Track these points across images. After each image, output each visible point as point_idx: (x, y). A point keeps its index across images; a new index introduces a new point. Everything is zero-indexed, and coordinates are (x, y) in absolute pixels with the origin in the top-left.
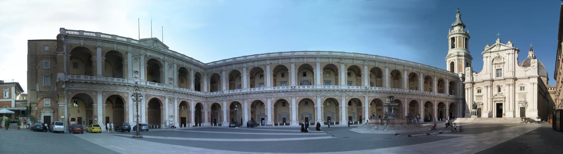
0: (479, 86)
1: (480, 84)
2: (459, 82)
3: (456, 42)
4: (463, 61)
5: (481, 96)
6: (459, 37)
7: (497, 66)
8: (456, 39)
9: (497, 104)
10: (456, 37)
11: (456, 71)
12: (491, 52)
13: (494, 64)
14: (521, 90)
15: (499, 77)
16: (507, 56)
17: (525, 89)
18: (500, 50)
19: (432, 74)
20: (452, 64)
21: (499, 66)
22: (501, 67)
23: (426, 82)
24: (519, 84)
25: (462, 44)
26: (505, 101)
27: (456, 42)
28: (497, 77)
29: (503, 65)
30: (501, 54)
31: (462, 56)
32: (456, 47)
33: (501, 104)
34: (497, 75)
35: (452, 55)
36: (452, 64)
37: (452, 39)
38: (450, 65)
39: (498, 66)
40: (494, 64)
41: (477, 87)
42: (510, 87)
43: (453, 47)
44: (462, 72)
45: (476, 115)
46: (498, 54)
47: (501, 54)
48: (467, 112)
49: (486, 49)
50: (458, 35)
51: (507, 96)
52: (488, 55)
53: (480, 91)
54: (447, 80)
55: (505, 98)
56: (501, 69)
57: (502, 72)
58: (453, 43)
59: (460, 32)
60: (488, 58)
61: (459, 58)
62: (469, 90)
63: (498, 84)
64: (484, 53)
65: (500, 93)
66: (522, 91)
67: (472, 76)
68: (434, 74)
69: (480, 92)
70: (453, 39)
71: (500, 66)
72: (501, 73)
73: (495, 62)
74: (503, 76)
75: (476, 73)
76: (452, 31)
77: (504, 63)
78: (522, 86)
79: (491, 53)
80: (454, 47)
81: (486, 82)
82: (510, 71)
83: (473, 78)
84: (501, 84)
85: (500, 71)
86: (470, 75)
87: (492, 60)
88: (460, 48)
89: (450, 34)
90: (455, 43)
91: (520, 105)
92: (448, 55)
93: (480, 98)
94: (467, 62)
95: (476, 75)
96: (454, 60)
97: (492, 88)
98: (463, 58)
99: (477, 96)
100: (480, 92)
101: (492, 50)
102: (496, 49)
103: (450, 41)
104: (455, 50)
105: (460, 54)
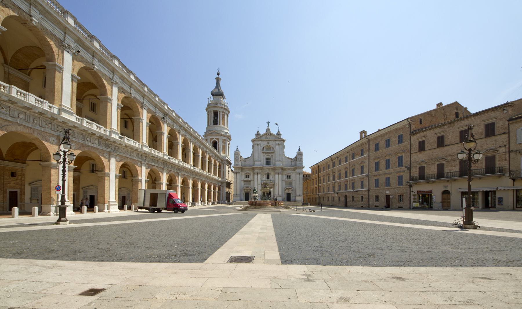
0: (248, 171)
2: (223, 165)
5: (250, 181)
7: (266, 154)
8: (220, 114)
10: (220, 112)
13: (263, 153)
14: (287, 178)
16: (277, 146)
17: (291, 178)
21: (269, 155)
28: (266, 165)
29: (272, 154)
32: (220, 125)
34: (266, 163)
39: (267, 154)
40: (263, 153)
41: (245, 173)
46: (268, 143)
53: (249, 176)
55: (274, 185)
60: (259, 146)
69: (249, 178)
72: (270, 161)
73: (265, 150)
74: (272, 165)
79: (262, 141)
85: (269, 160)
87: (262, 148)
93: (248, 183)
96: (218, 139)
99: (245, 181)
100: (249, 178)
102: (266, 138)
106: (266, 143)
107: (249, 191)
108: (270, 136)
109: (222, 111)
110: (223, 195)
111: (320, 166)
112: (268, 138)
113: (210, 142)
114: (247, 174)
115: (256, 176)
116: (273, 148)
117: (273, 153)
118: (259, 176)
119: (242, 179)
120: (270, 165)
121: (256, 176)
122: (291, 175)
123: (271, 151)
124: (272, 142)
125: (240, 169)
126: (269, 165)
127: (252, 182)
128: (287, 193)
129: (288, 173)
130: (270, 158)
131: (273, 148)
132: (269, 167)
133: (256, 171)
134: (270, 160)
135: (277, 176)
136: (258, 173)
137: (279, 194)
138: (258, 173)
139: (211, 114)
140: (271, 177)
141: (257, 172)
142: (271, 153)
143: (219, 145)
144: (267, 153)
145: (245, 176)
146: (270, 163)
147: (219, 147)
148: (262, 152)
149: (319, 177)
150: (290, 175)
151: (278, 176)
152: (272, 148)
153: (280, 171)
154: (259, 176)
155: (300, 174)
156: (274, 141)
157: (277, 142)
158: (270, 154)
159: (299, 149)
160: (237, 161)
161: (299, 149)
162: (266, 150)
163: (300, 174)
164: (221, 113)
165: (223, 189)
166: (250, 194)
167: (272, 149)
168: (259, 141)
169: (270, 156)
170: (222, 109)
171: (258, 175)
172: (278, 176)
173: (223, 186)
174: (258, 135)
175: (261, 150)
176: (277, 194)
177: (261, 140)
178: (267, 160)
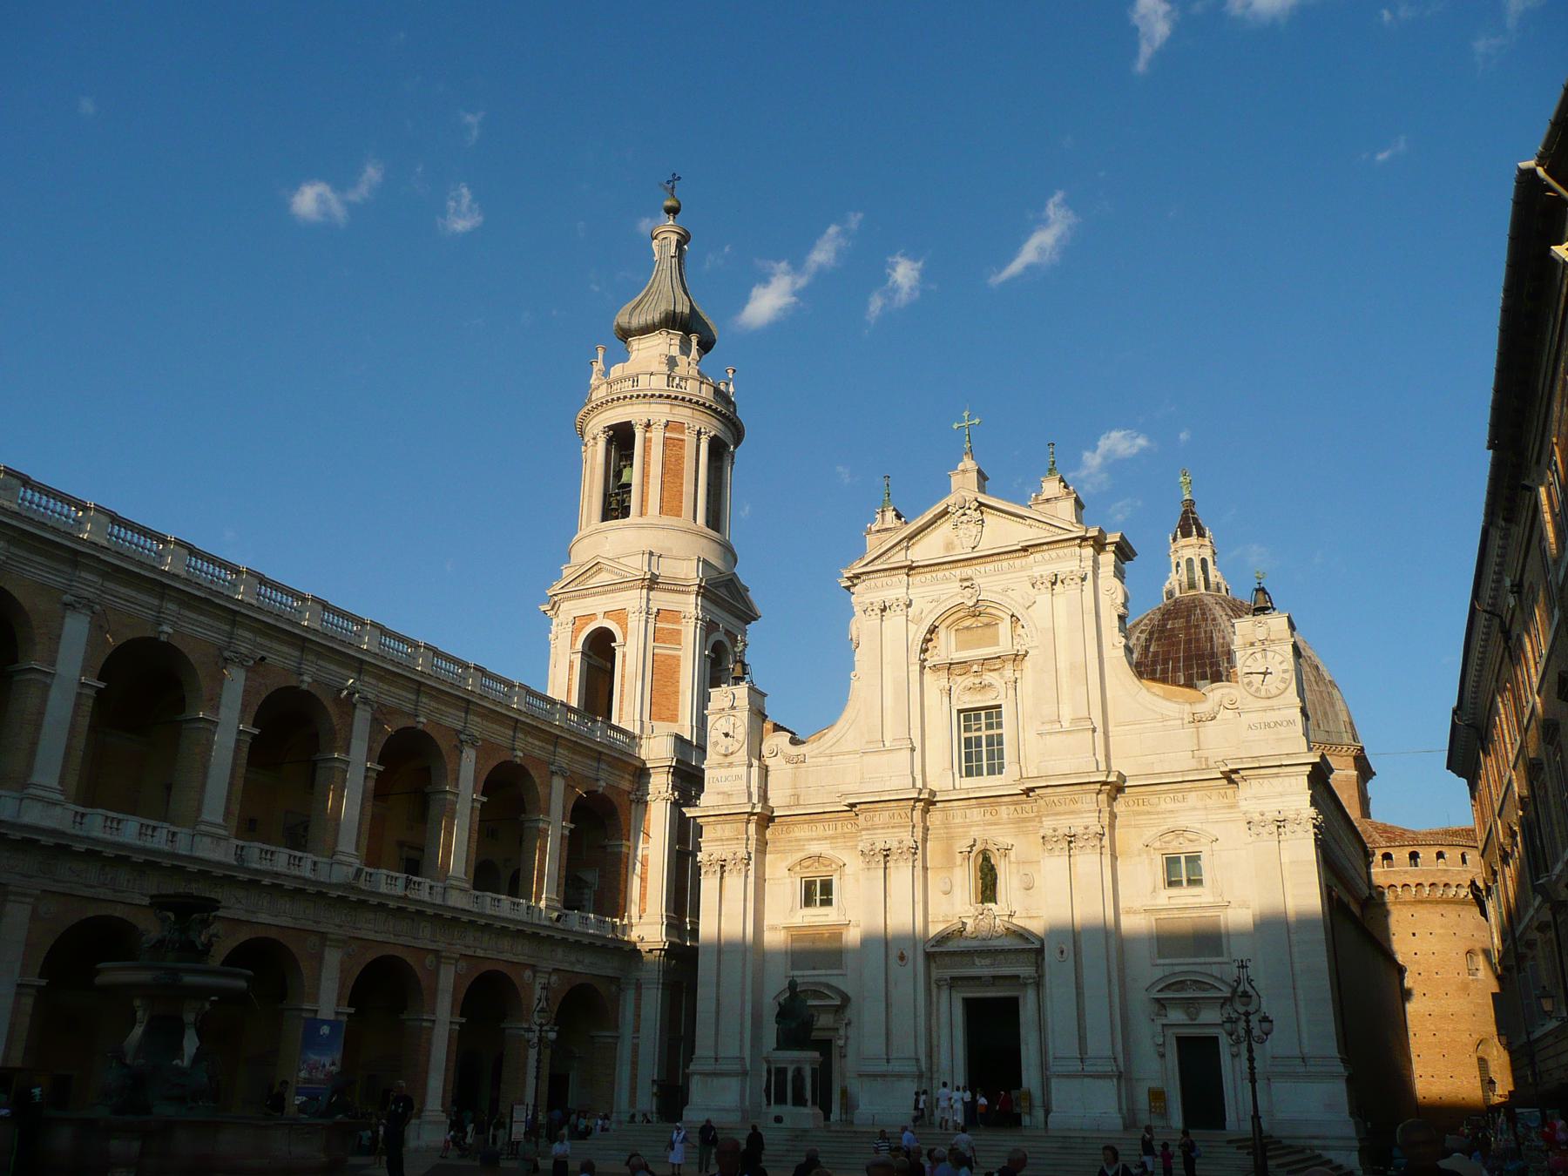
0: (815, 848)
1: (819, 830)
4: (690, 633)
6: (667, 425)
8: (647, 441)
9: (968, 1003)
11: (627, 710)
12: (910, 569)
13: (935, 668)
15: (980, 774)
16: (1043, 597)
18: (985, 547)
19: (448, 721)
20: (600, 649)
23: (381, 790)
24: (1149, 834)
25: (688, 488)
26: (1039, 983)
28: (969, 773)
29: (1008, 672)
30: (992, 583)
31: (677, 588)
33: (1010, 1008)
34: (968, 757)
35: (604, 577)
36: (600, 649)
37: (609, 442)
38: (577, 659)
39: (970, 680)
40: (935, 668)
41: (802, 855)
43: (616, 505)
44: (673, 718)
45: (804, 1104)
47: (992, 583)
48: (708, 1068)
49: (874, 545)
50: (661, 413)
52: (893, 589)
53: (827, 887)
54: (558, 785)
56: (999, 706)
57: (1007, 731)
58: (619, 475)
59: (673, 392)
60: (895, 620)
61: (661, 600)
62: (734, 882)
63: (975, 832)
64: (857, 576)
65: (991, 905)
67: (760, 757)
68: (459, 726)
69: (827, 902)
70: (621, 439)
71: (990, 685)
72: (1001, 735)
73: (947, 647)
74: (1010, 770)
75: (795, 741)
76: (617, 370)
77: (1018, 658)
78: (1182, 847)
79: (916, 579)
80: (625, 512)
81: (882, 817)
82: (1066, 724)
83: (765, 771)
84: (1000, 836)
85: (989, 726)
86: (742, 755)
88: (667, 520)
89: (600, 394)
90: (634, 475)
91: (1176, 1016)
92: (568, 572)
94: (716, 637)
95: (795, 750)
96: (620, 615)
97: (925, 869)
98: (690, 605)
100: (827, 902)
101: (925, 550)
102: (949, 546)
103: (595, 454)
104: (630, 534)
105: (666, 569)
106: (955, 586)
110: (634, 1064)
113: (572, 645)
114: (809, 874)
117: (1018, 658)
122: (1204, 848)
126: (991, 772)
128: (1182, 1042)
130: (994, 711)
132: (985, 783)
134: (1000, 725)
137: (1091, 1050)
140: (1007, 881)
141: (880, 845)
143: (624, 656)
147: (623, 676)
150: (1191, 848)
153: (1086, 815)
156: (1017, 562)
158: (989, 677)
160: (730, 765)
165: (638, 1007)
167: (1004, 627)
169: (997, 689)
170: (666, 408)
173: (639, 987)
178: (979, 729)
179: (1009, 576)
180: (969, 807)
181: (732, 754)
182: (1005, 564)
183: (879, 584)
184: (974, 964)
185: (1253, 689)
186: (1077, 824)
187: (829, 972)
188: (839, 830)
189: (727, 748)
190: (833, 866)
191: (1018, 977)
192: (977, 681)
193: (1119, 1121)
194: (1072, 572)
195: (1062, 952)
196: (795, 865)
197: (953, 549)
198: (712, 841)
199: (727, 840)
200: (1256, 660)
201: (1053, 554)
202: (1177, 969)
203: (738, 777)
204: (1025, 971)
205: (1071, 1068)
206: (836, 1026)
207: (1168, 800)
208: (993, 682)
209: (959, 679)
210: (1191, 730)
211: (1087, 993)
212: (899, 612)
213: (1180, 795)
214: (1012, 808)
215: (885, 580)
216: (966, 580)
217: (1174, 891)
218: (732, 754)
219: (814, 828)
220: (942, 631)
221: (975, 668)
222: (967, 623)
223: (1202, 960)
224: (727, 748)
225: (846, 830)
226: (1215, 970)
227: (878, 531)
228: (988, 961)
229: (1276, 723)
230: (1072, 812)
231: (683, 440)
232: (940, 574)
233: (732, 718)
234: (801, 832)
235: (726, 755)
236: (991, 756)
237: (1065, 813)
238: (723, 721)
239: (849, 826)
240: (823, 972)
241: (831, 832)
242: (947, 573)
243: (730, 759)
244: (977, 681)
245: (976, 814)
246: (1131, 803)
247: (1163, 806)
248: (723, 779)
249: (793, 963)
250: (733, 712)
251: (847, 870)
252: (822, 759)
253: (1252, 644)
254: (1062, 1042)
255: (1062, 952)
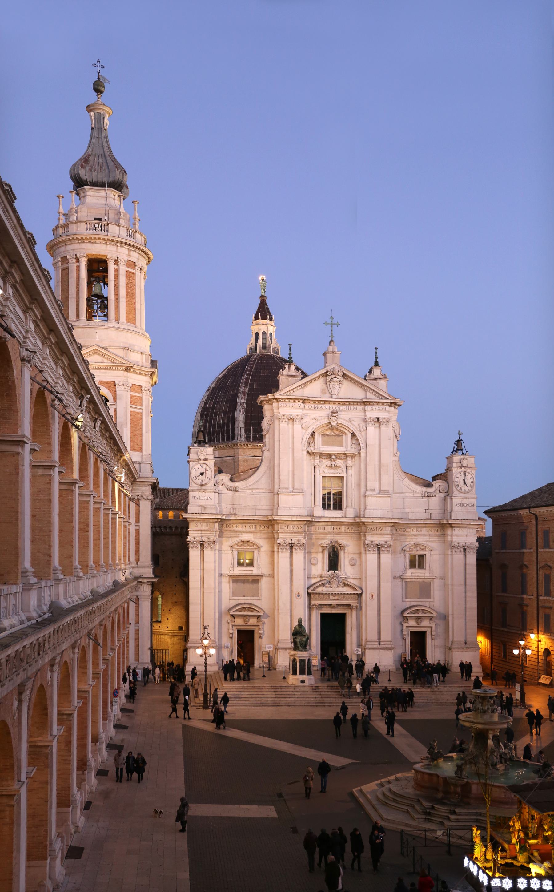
0: (245, 537)
1: (247, 528)
3: (117, 287)
5: (256, 580)
8: (117, 271)
9: (323, 615)
10: (117, 262)
16: (372, 430)
17: (427, 565)
22: (339, 471)
26: (359, 608)
27: (117, 287)
29: (350, 462)
32: (117, 320)
33: (340, 619)
39: (327, 462)
41: (239, 539)
42: (382, 555)
51: (370, 586)
52: (296, 410)
60: (297, 426)
66: (417, 573)
71: (339, 466)
93: (248, 586)
107: (253, 621)
108: (340, 383)
109: (126, 258)
111: (545, 520)
112: (335, 392)
115: (283, 557)
116: (353, 435)
117: (353, 456)
118: (299, 556)
119: (225, 571)
120: (340, 507)
121: (283, 557)
122: (427, 552)
123: (348, 447)
124: (348, 410)
125: (217, 525)
126: (335, 508)
127: (264, 583)
129: (416, 545)
131: (353, 435)
133: (284, 537)
135: (371, 557)
136: (291, 546)
137: (382, 638)
138: (291, 546)
139: (78, 268)
142: (346, 456)
144: (329, 456)
145: (235, 552)
146: (340, 500)
148: (308, 452)
149: (541, 565)
150: (421, 552)
151: (379, 558)
152: (349, 435)
154: (299, 556)
155: (465, 550)
156: (358, 407)
157: (372, 412)
158: (339, 462)
159: (459, 442)
160: (205, 491)
161: (459, 442)
162: (325, 444)
163: (465, 550)
164: (123, 269)
166: (256, 636)
168: (296, 404)
170: (126, 251)
171: (294, 554)
172: (379, 558)
174: (290, 378)
175: (305, 441)
176: (376, 638)
177: (305, 401)
179: (353, 413)
180: (327, 525)
181: (206, 484)
182: (352, 407)
183: (288, 405)
184: (329, 599)
185: (459, 488)
186: (382, 539)
187: (252, 598)
188: (258, 529)
189: (202, 481)
190: (255, 546)
191: (350, 605)
192: (333, 463)
193: (395, 667)
194: (384, 418)
195: (372, 596)
196: (234, 545)
197: (326, 393)
198: (196, 531)
199: (204, 531)
200: (461, 475)
201: (377, 407)
202: (413, 604)
203: (210, 498)
204: (353, 603)
205: (375, 646)
206: (258, 624)
207: (414, 530)
208: (340, 464)
209: (324, 461)
210: (425, 500)
211: (382, 614)
212: (297, 422)
213: (419, 529)
214: (347, 527)
215: (292, 403)
216: (335, 413)
217: (413, 571)
218: (206, 484)
219: (244, 527)
220: (317, 436)
221: (333, 457)
222: (329, 432)
223: (422, 600)
224: (202, 481)
225: (261, 529)
226: (427, 604)
227: (287, 375)
228: (336, 598)
229: (467, 505)
230: (380, 534)
231: (134, 274)
232: (319, 406)
233: (204, 466)
234: (237, 528)
235: (202, 485)
236: (329, 499)
237: (377, 534)
238: (199, 466)
239: (263, 527)
240: (249, 598)
241: (253, 529)
242: (323, 406)
243: (204, 488)
244: (333, 463)
245: (329, 528)
246: (398, 530)
247: (412, 533)
248: (201, 498)
249: (233, 593)
250: (205, 462)
251: (262, 549)
252: (247, 491)
253: (461, 468)
254: (370, 634)
255: (372, 596)
